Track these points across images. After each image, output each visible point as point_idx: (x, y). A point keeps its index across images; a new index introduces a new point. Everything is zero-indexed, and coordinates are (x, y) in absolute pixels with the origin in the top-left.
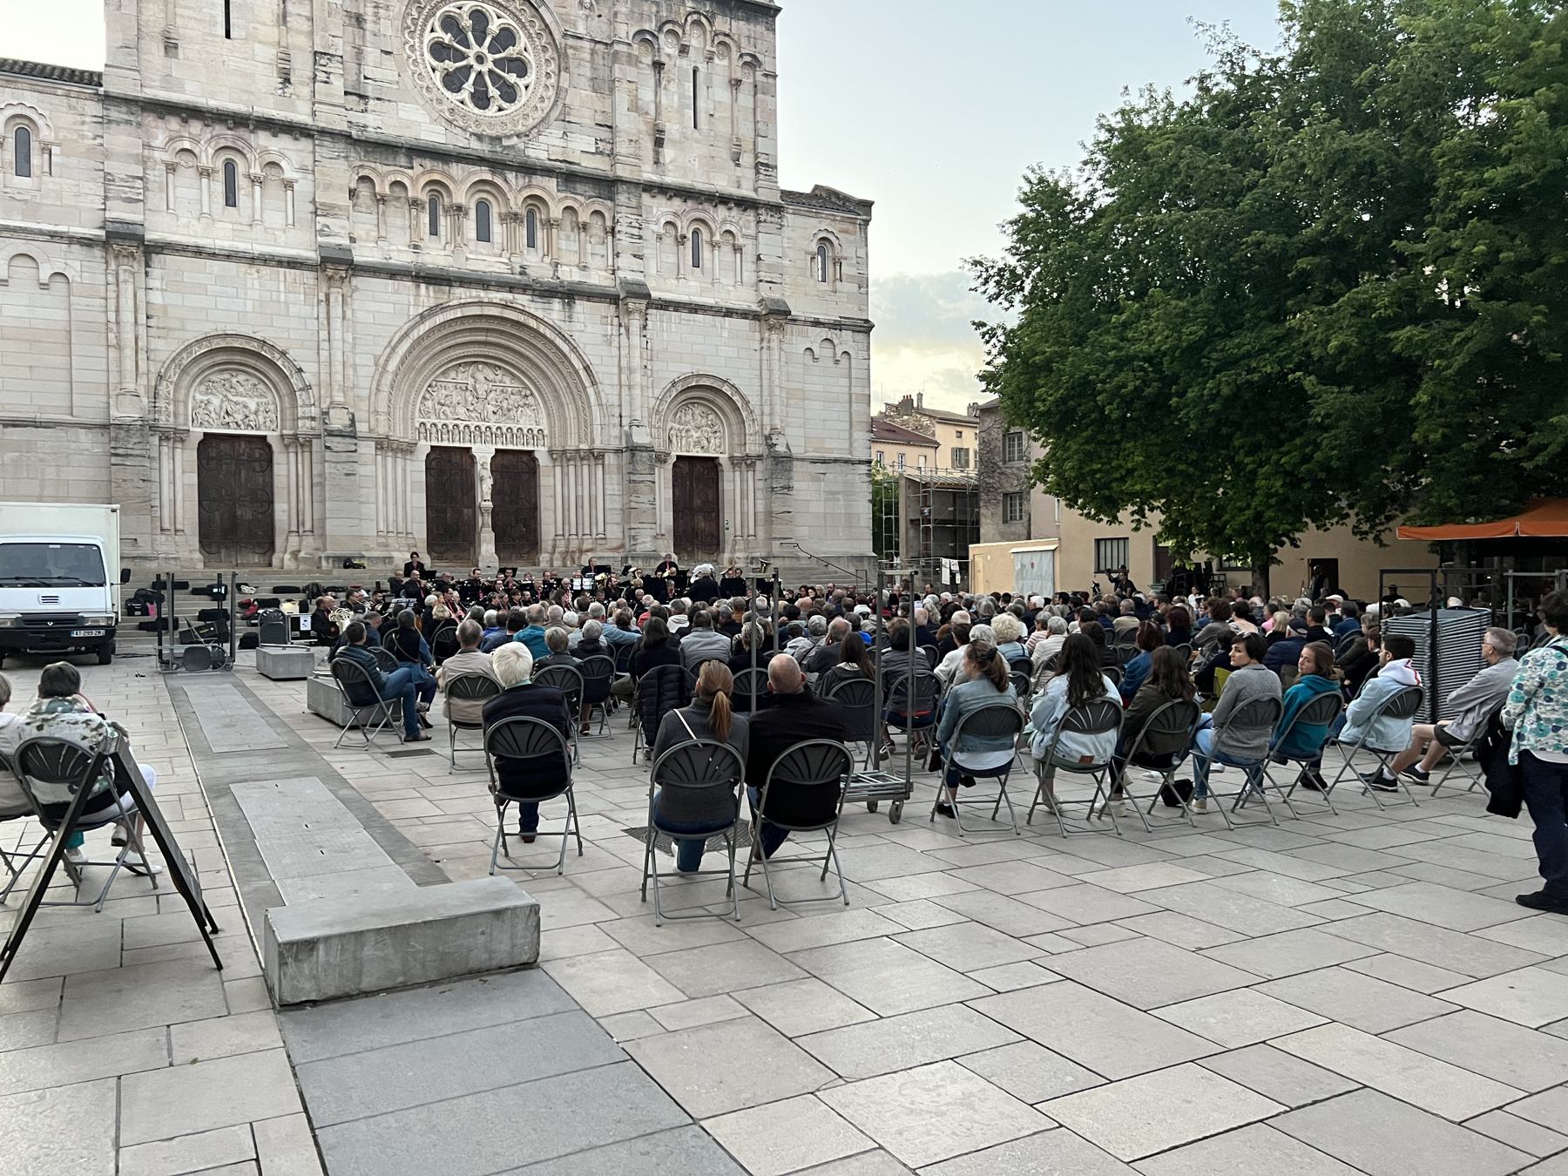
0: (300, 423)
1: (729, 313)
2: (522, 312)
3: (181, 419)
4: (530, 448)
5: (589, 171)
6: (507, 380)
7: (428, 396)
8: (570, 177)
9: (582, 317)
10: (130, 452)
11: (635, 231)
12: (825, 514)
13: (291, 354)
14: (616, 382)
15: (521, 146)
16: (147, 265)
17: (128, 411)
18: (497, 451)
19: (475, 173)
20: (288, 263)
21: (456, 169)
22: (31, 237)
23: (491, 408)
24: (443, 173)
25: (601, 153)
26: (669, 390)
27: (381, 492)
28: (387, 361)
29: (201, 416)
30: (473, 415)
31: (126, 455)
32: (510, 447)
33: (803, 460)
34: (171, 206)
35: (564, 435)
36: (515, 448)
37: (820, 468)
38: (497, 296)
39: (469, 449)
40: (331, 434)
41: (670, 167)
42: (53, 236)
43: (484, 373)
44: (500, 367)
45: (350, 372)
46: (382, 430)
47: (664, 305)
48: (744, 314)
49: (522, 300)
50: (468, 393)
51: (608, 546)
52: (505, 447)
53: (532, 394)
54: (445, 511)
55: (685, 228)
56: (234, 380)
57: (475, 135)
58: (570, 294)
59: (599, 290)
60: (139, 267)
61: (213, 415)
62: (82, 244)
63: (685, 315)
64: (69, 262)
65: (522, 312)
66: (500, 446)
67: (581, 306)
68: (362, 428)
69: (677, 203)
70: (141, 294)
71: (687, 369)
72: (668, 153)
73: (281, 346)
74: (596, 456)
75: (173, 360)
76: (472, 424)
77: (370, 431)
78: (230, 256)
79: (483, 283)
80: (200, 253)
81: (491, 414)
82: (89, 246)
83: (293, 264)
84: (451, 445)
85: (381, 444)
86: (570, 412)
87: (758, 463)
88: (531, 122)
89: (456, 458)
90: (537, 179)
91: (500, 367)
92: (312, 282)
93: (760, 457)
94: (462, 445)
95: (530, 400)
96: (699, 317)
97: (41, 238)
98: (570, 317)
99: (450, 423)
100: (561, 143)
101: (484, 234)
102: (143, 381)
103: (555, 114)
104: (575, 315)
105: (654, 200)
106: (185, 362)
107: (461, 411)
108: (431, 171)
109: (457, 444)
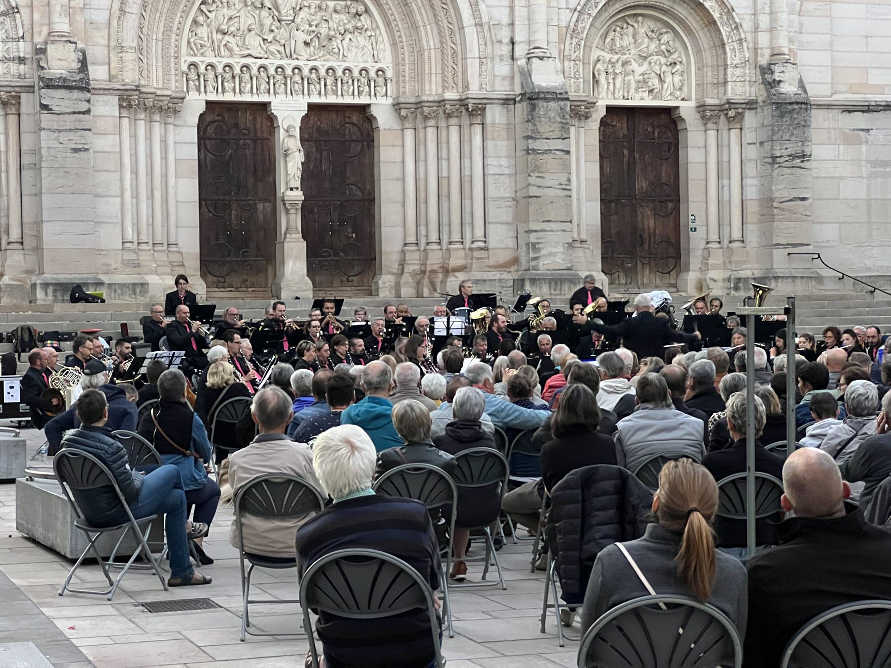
4: (363, 100)
7: (201, 19)
12: (869, 201)
18: (312, 107)
23: (301, 37)
27: (128, 177)
30: (273, 48)
32: (332, 99)
33: (829, 107)
35: (419, 76)
36: (340, 100)
37: (860, 120)
39: (265, 106)
40: (50, 84)
46: (130, 77)
50: (265, 13)
51: (492, 262)
52: (323, 100)
53: (367, 11)
54: (227, 207)
66: (316, 99)
68: (98, 73)
76: (272, 64)
81: (301, 45)
84: (238, 98)
86: (429, 39)
87: (748, 115)
89: (245, 120)
93: (751, 105)
94: (255, 99)
95: (365, 21)
99: (237, 63)
107: (254, 42)
109: (247, 98)
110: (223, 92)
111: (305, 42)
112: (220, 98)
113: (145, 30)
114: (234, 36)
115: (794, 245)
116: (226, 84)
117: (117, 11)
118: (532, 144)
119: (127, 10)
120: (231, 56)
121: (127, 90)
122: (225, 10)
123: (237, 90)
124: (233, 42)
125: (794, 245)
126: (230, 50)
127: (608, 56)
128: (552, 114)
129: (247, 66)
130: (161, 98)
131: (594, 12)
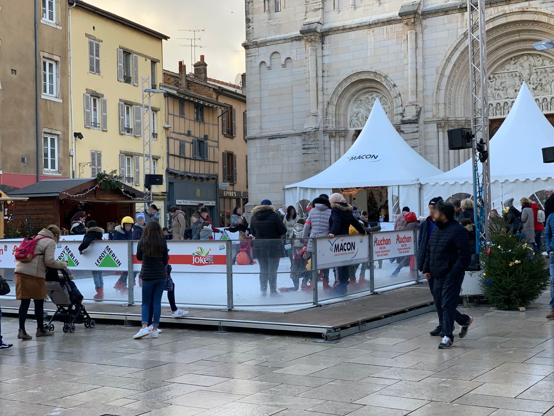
0: (395, 118)
2: (536, 13)
3: (342, 125)
6: (547, 62)
10: (310, 146)
13: (390, 77)
16: (323, 43)
17: (310, 125)
20: (388, 21)
22: (277, 42)
28: (444, 69)
29: (355, 121)
31: (308, 148)
34: (336, 6)
42: (285, 40)
43: (525, 62)
44: (540, 55)
45: (420, 81)
46: (442, 115)
56: (370, 97)
60: (318, 45)
61: (361, 120)
62: (297, 40)
64: (292, 51)
65: (536, 13)
70: (319, 60)
73: (384, 73)
75: (334, 93)
77: (434, 116)
78: (359, 27)
80: (345, 29)
82: (300, 40)
83: (389, 22)
85: (440, 124)
91: (540, 55)
92: (401, 29)
97: (281, 42)
102: (320, 106)
106: (340, 93)
110: (496, 114)
111: (533, 88)
112: (495, 117)
113: (452, 95)
114: (502, 90)
116: (497, 111)
117: (436, 90)
119: (441, 88)
120: (501, 99)
121: (439, 121)
122: (500, 80)
123: (502, 113)
126: (500, 96)
129: (507, 103)
130: (461, 121)
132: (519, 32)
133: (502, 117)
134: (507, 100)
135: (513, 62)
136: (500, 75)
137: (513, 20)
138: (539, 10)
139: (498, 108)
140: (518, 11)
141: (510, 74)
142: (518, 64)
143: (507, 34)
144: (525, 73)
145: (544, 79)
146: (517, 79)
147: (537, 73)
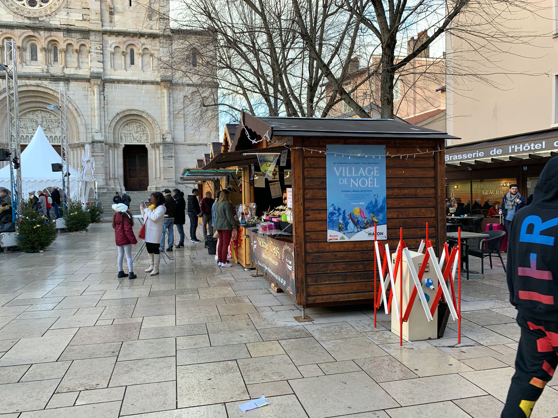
1: (144, 83)
2: (46, 88)
5: (80, 28)
6: (52, 116)
8: (68, 31)
9: (73, 88)
11: (99, 51)
14: (90, 115)
15: (48, 20)
19: (25, 32)
21: (18, 32)
24: (11, 34)
25: (85, 20)
26: (115, 117)
33: (183, 144)
37: (193, 148)
38: (33, 82)
41: (117, 23)
44: (48, 112)
47: (113, 81)
48: (152, 83)
49: (46, 83)
55: (123, 48)
57: (26, 17)
58: (67, 79)
59: (82, 77)
63: (123, 85)
65: (46, 88)
67: (73, 84)
69: (121, 39)
71: (125, 108)
72: (116, 17)
74: (83, 146)
79: (27, 77)
88: (53, 10)
90: (53, 33)
91: (48, 112)
93: (160, 144)
96: (130, 85)
98: (68, 89)
100: (67, 17)
101: (34, 57)
103: (63, 5)
104: (70, 88)
105: (109, 38)
108: (6, 33)
115: (170, 179)
118: (94, 154)
124: (24, 130)
125: (170, 179)
127: (126, 132)
128: (98, 146)
131: (116, 121)
132: (35, 96)
133: (25, 144)
134: (28, 135)
135: (31, 113)
136: (23, 120)
137: (32, 89)
138: (48, 87)
139: (22, 138)
140: (34, 84)
141: (30, 120)
142: (35, 115)
143: (28, 97)
144: (39, 121)
145: (50, 125)
146: (34, 124)
147: (46, 121)
